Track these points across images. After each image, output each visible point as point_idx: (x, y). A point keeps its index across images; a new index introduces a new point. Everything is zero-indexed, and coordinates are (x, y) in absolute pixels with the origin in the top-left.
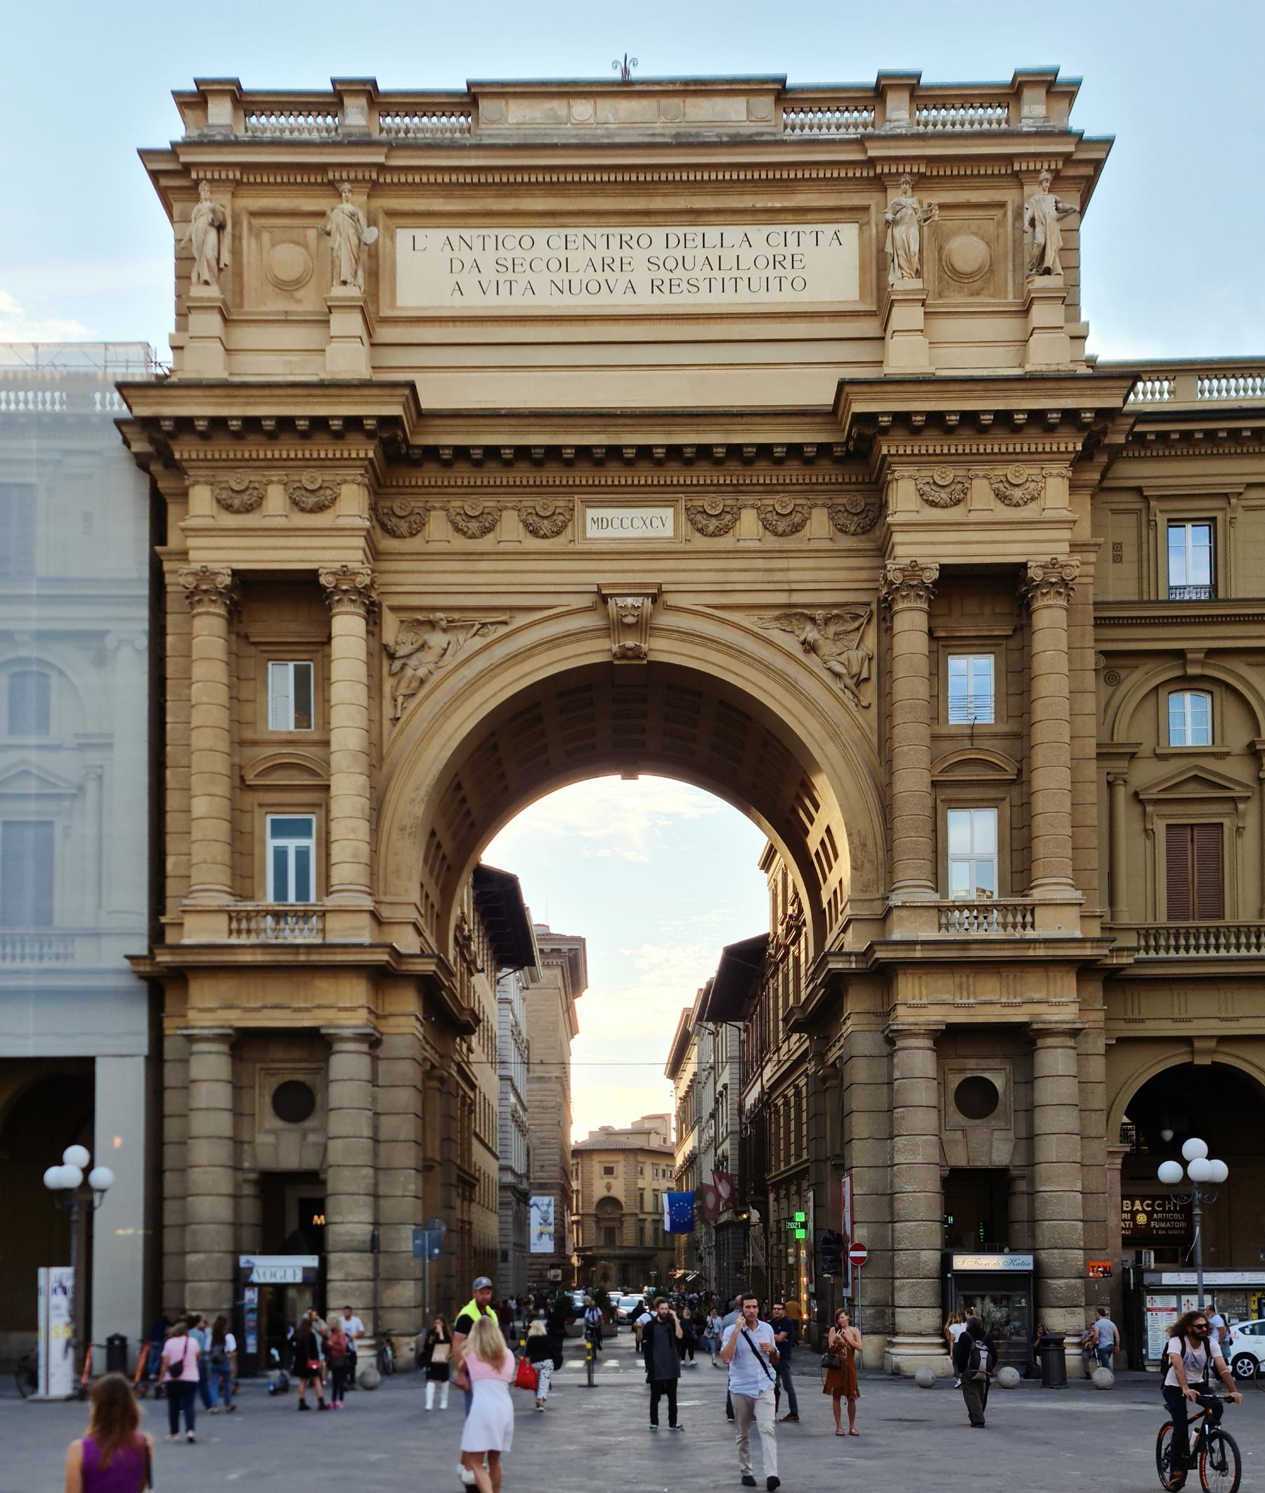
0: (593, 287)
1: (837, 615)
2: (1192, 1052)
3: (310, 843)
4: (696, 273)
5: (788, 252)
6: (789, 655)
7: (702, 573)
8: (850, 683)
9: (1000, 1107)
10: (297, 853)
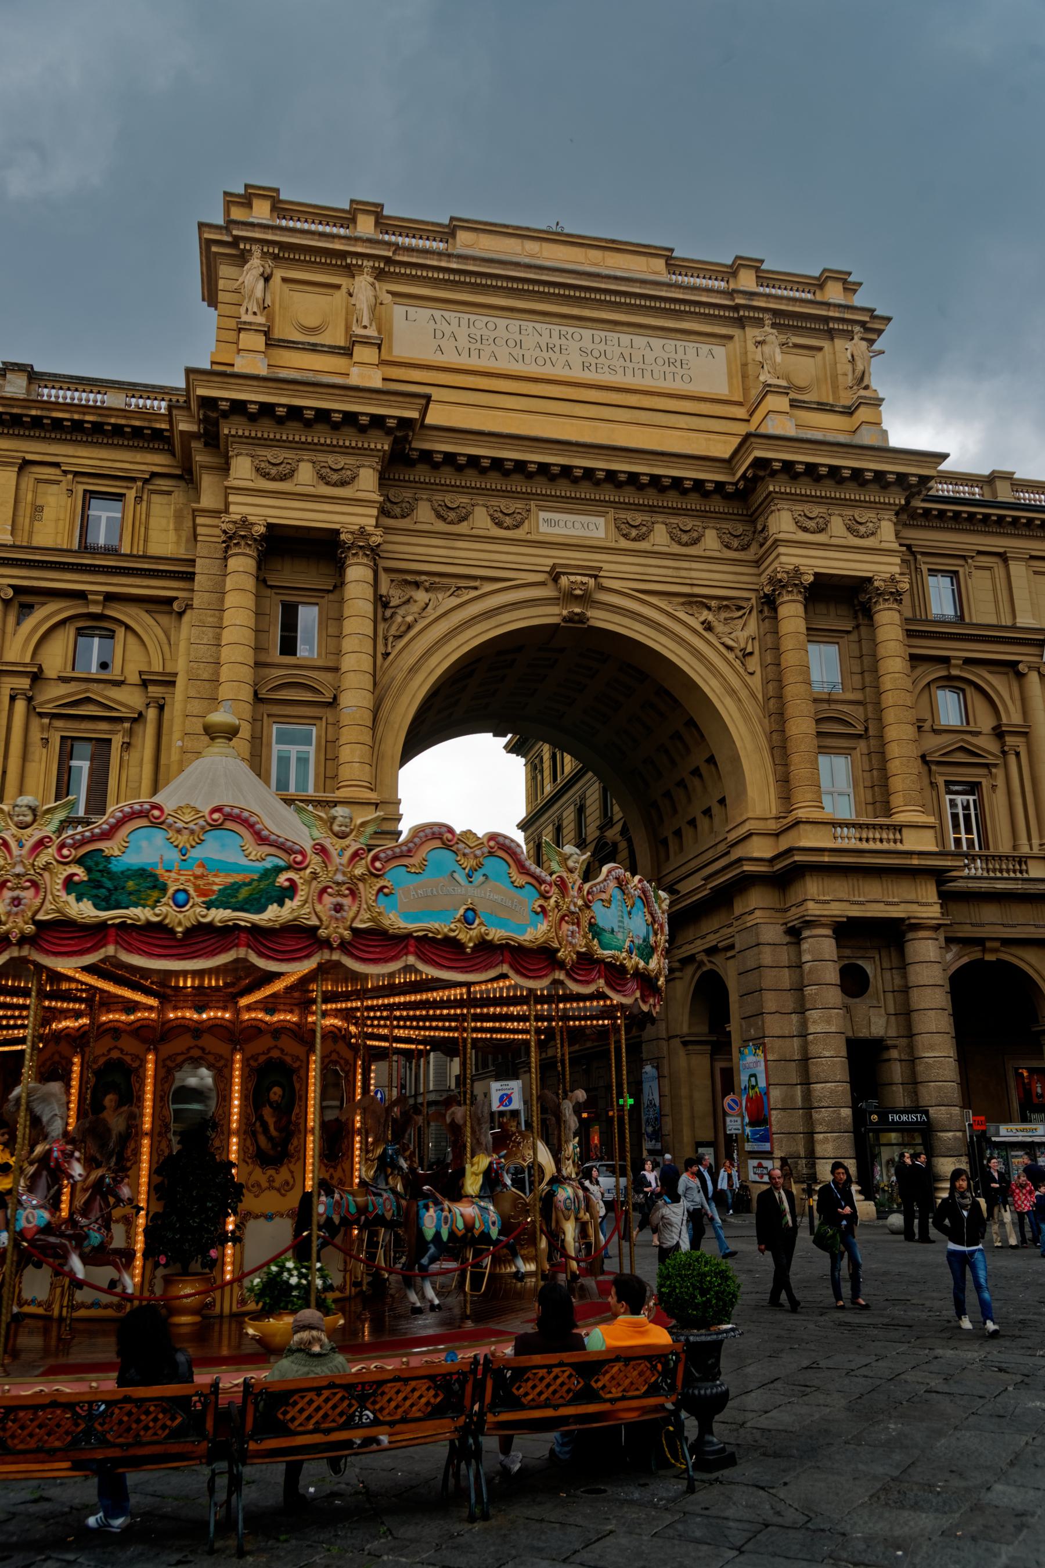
0: (541, 362)
1: (727, 606)
2: (984, 951)
3: (311, 750)
4: (614, 362)
5: (678, 357)
6: (694, 631)
7: (629, 566)
8: (740, 654)
9: (871, 989)
10: (299, 759)
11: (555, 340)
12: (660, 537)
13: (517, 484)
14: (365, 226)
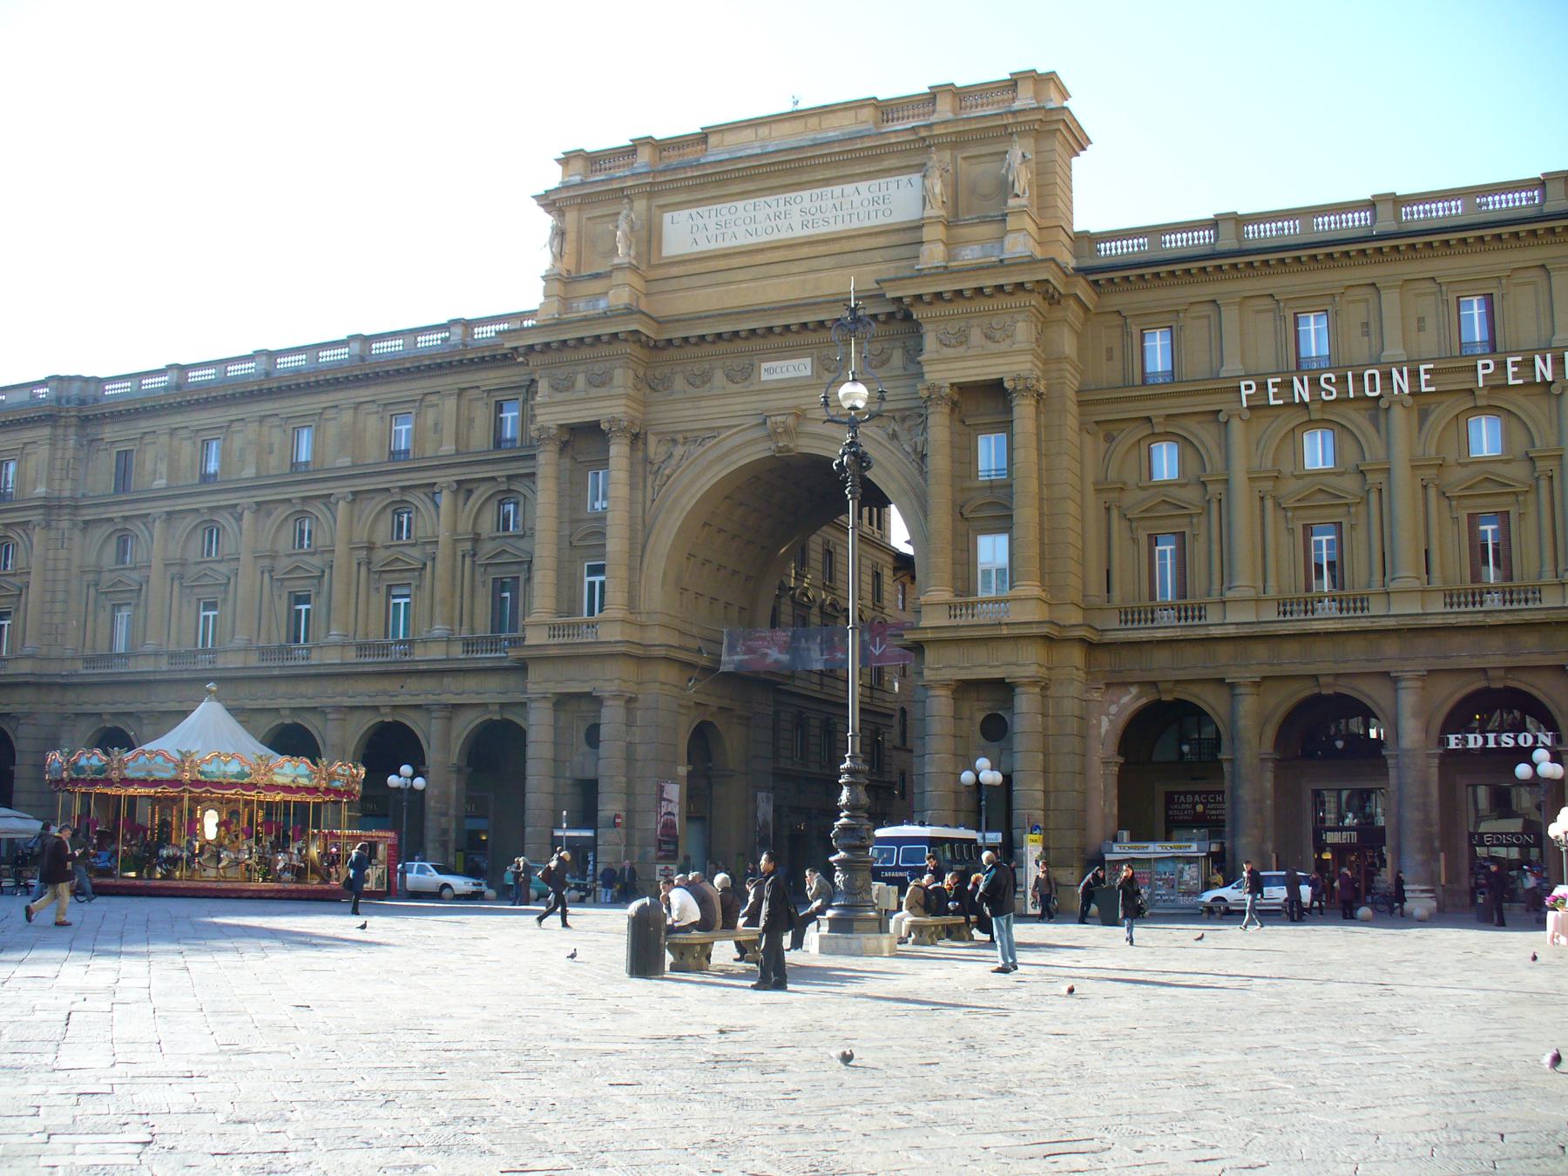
11: (782, 208)
13: (740, 345)
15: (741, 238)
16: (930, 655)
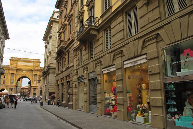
12: (29, 72)
14: (17, 58)
15: (22, 64)
16: (33, 87)
